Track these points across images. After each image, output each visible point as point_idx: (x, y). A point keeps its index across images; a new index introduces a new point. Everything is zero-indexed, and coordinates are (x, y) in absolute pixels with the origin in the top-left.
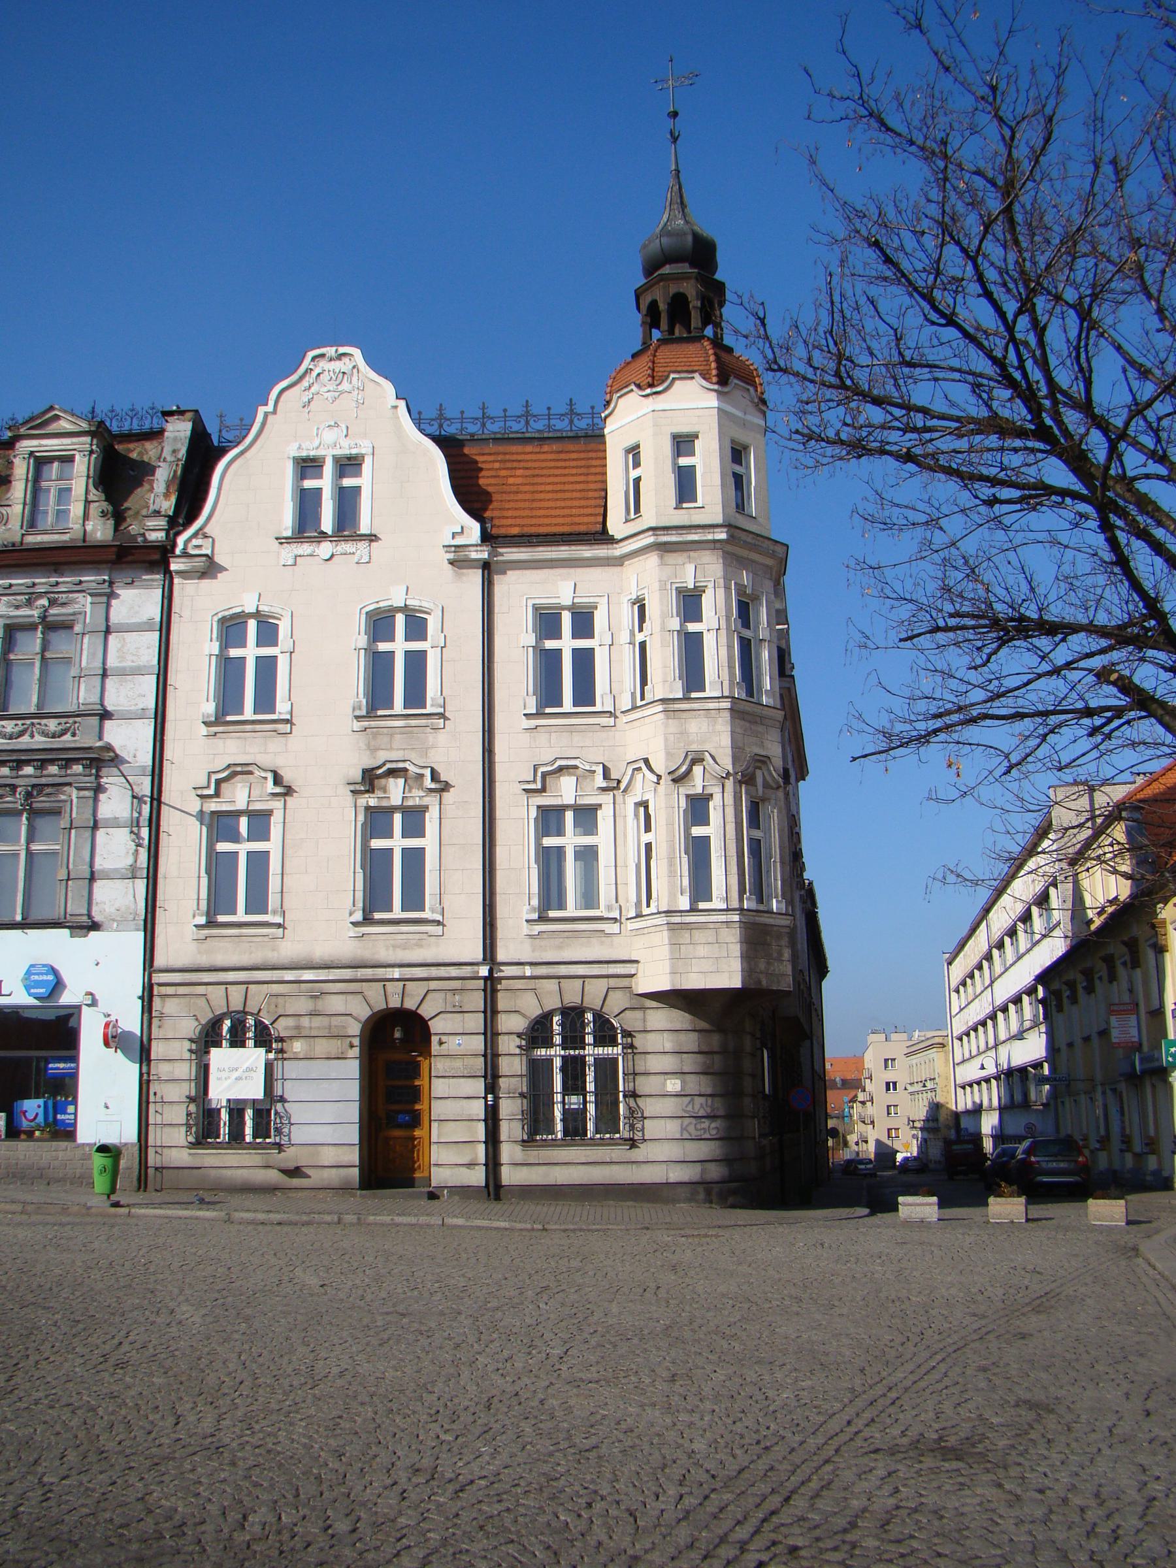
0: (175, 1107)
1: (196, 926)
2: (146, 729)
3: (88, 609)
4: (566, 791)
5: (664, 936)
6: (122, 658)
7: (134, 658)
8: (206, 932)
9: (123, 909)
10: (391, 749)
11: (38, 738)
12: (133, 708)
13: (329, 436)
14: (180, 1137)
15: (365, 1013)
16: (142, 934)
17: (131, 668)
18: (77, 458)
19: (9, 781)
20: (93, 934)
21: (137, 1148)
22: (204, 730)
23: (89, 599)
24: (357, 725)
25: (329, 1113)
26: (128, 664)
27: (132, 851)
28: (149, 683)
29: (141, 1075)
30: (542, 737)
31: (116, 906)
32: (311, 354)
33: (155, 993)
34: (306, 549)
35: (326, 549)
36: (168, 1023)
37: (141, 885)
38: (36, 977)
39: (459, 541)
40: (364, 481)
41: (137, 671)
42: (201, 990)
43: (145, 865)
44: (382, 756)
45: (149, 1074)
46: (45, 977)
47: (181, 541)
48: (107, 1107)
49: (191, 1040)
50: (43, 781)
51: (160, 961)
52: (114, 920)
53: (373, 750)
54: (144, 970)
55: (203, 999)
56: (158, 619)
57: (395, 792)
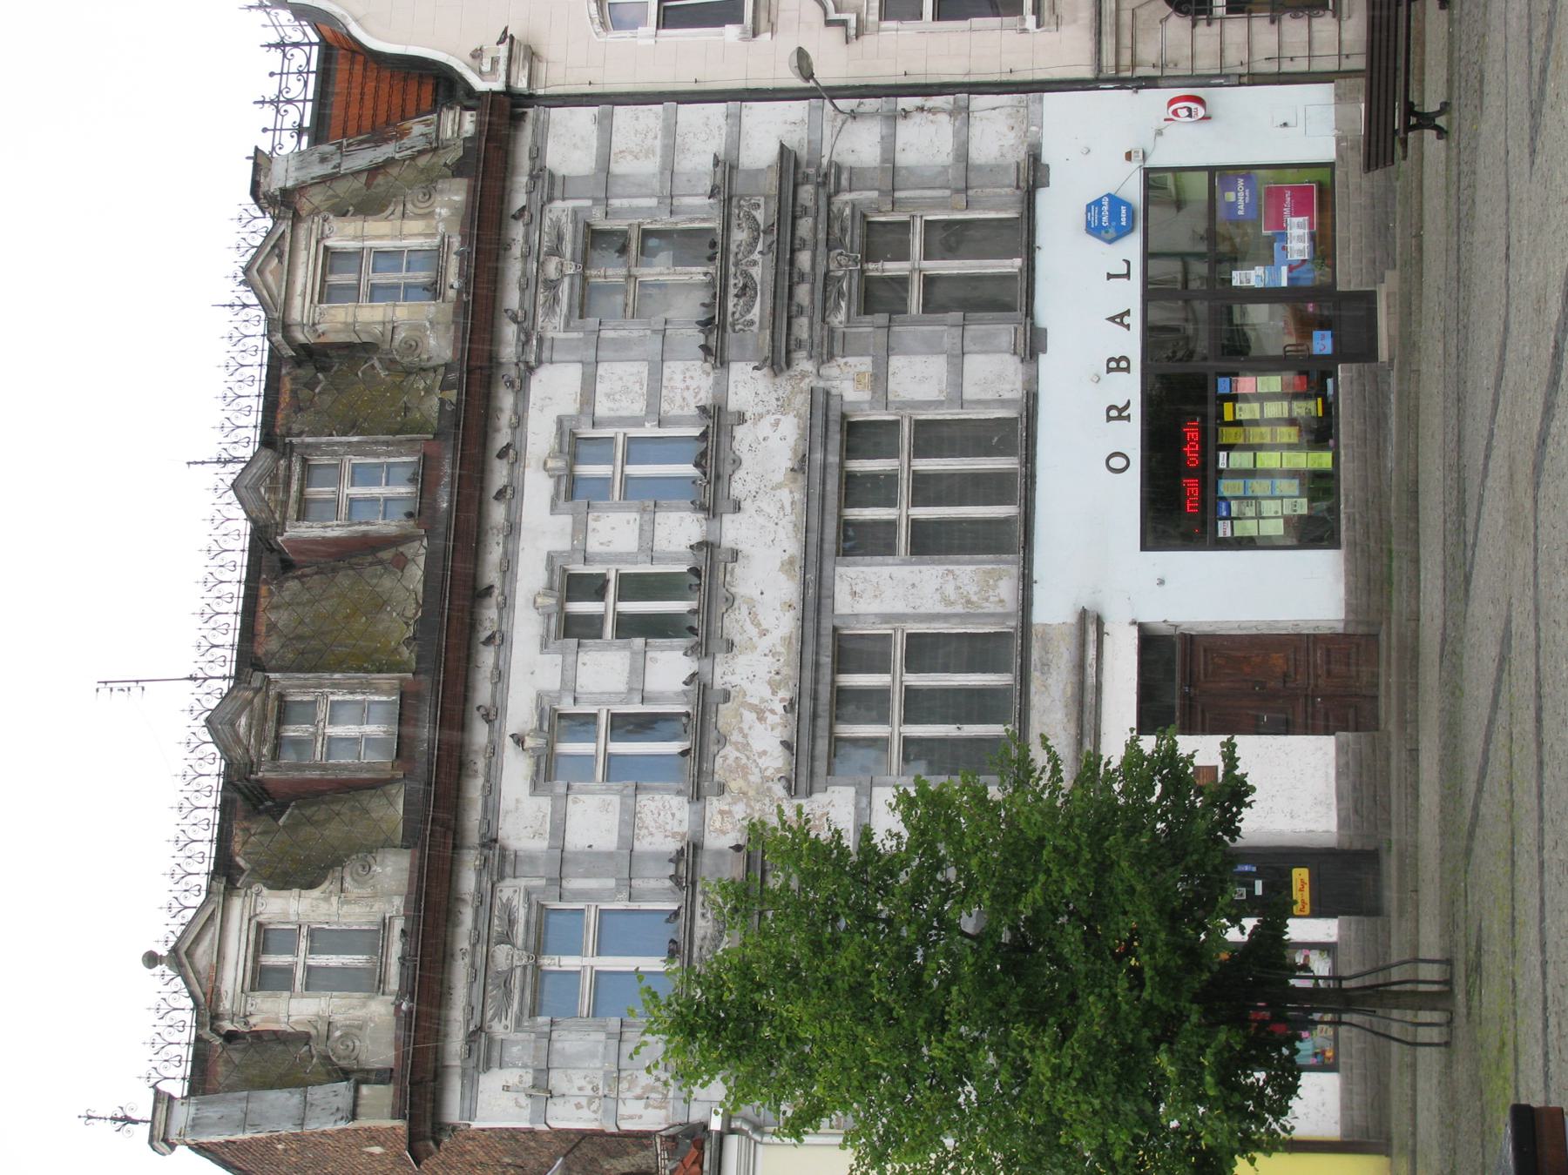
0: (1286, 39)
1: (1038, 26)
2: (756, 112)
3: (570, 204)
6: (649, 152)
7: (650, 135)
8: (1046, 13)
9: (1011, 122)
12: (724, 132)
14: (1325, 26)
16: (1047, 95)
17: (664, 137)
18: (329, 243)
19: (820, 284)
20: (1046, 158)
21: (1342, 82)
22: (765, 37)
23: (558, 204)
26: (658, 143)
27: (930, 116)
28: (687, 112)
29: (1240, 84)
31: (1005, 130)
33: (1128, 74)
36: (1170, 55)
37: (980, 102)
38: (1105, 219)
41: (670, 130)
42: (1126, 17)
43: (951, 98)
45: (1241, 76)
46: (1105, 208)
47: (480, 85)
48: (1285, 124)
49: (1194, 26)
50: (822, 236)
51: (1086, 72)
52: (1025, 133)
54: (1098, 89)
55: (1138, 12)
56: (595, 110)
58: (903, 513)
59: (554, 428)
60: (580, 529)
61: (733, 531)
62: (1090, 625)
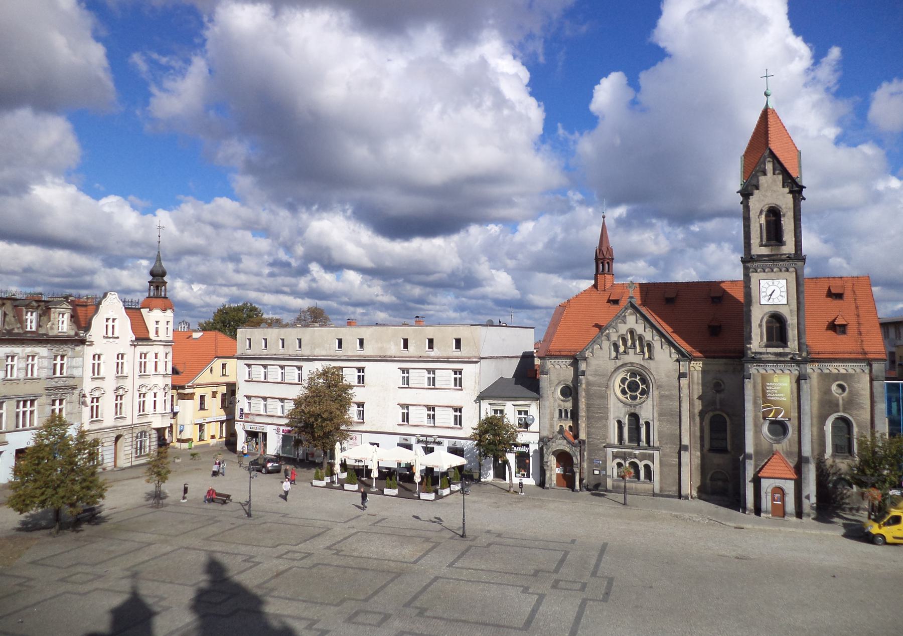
4: (143, 390)
5: (160, 418)
10: (120, 383)
11: (62, 382)
13: (111, 313)
15: (115, 436)
24: (116, 378)
25: (109, 456)
30: (141, 379)
32: (109, 293)
34: (108, 340)
35: (111, 340)
39: (132, 339)
40: (116, 323)
44: (119, 385)
47: (87, 336)
53: (117, 383)
57: (121, 392)
58: (21, 409)
59: (38, 352)
60: (23, 358)
61: (21, 383)
62: (5, 443)
